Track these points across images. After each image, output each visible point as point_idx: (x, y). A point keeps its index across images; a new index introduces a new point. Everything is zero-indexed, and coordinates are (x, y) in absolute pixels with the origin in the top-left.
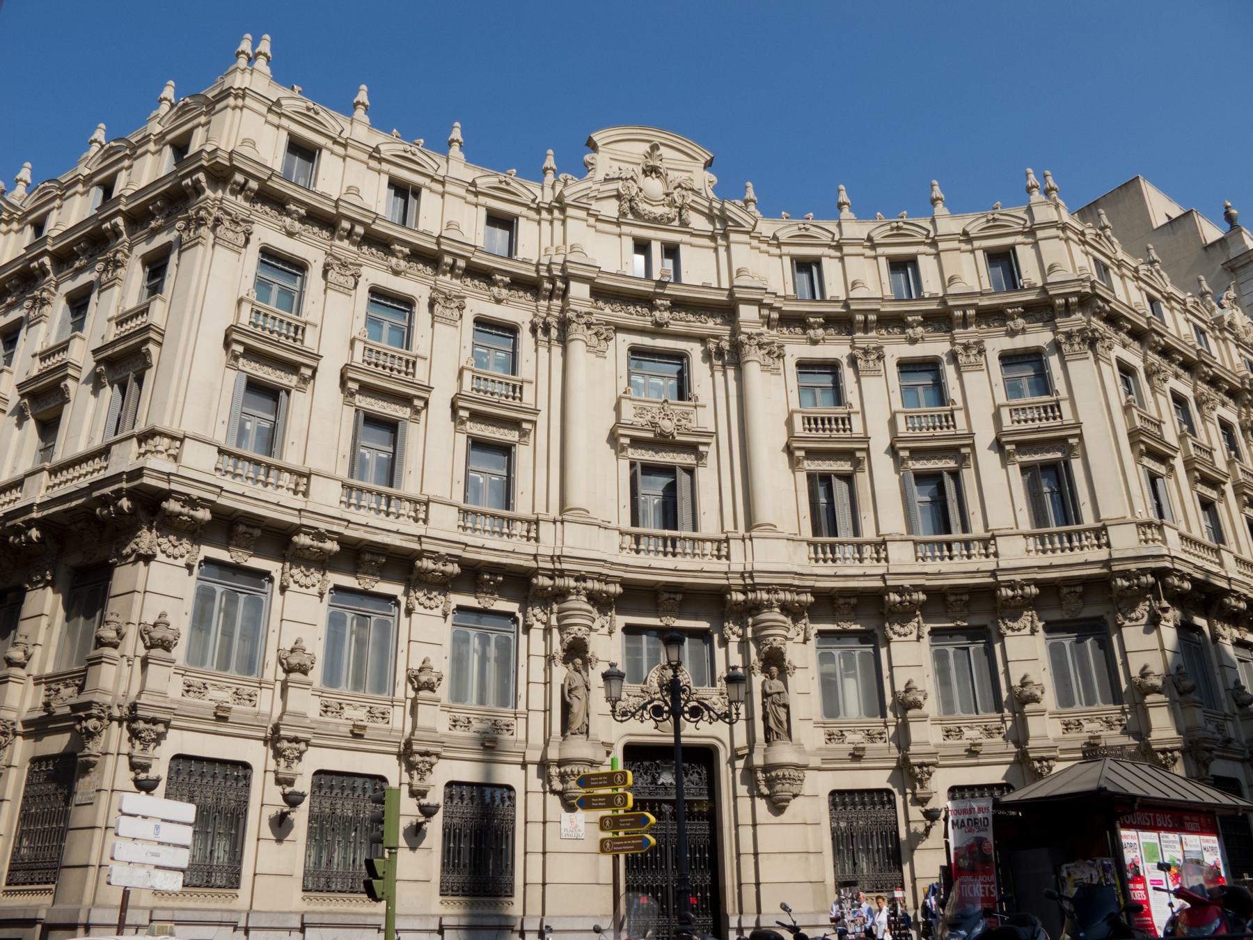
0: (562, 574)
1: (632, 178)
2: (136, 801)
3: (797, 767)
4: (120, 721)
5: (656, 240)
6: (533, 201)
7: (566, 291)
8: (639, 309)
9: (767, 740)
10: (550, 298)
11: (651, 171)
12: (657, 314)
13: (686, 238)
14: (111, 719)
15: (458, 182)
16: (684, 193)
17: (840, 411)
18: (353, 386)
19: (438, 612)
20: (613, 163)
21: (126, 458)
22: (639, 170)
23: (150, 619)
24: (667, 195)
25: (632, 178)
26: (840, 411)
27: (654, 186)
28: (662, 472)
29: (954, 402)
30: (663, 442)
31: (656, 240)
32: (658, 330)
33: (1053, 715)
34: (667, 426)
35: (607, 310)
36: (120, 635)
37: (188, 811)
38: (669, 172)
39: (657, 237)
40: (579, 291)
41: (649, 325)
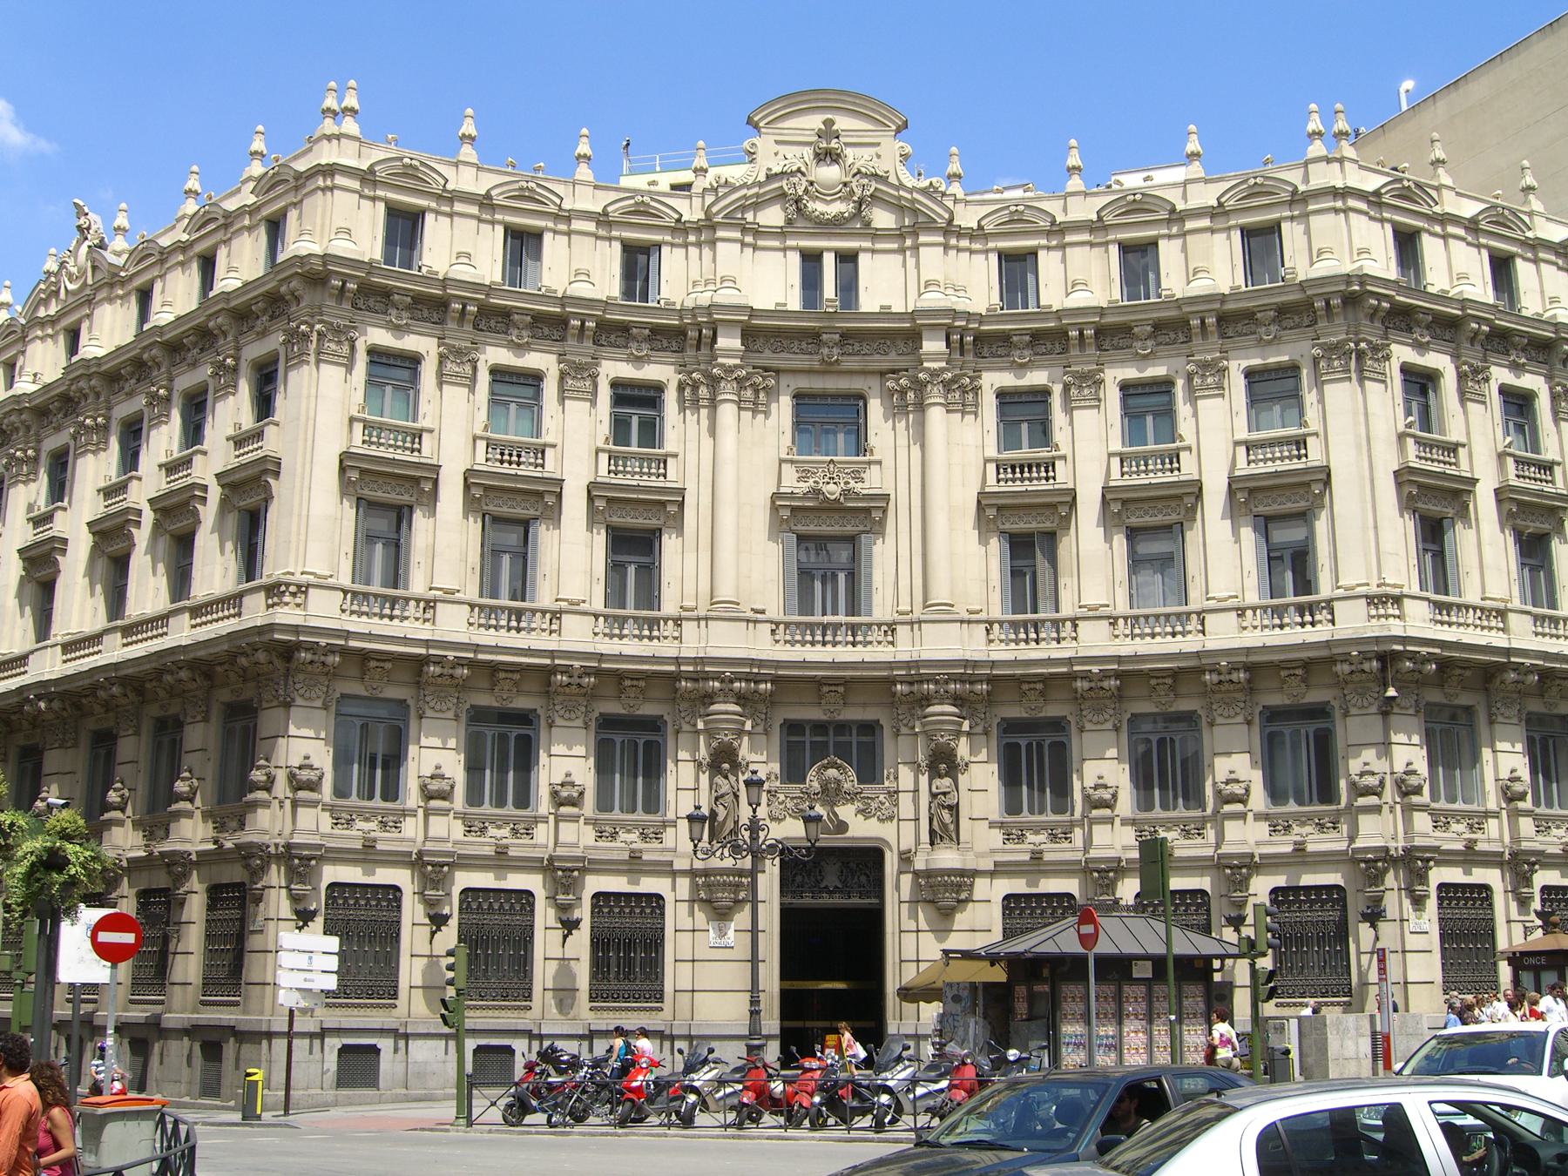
0: (707, 677)
1: (799, 170)
2: (289, 937)
3: (962, 873)
4: (278, 858)
5: (829, 250)
6: (678, 221)
7: (714, 340)
8: (804, 345)
9: (932, 844)
10: (698, 348)
11: (828, 156)
12: (825, 351)
13: (867, 244)
14: (270, 855)
15: (586, 215)
16: (865, 181)
17: (1043, 453)
18: (477, 493)
19: (579, 722)
20: (783, 149)
21: (256, 612)
22: (808, 153)
23: (295, 761)
24: (845, 184)
25: (799, 170)
26: (1043, 453)
27: (830, 173)
28: (828, 542)
29: (1182, 439)
30: (831, 508)
31: (829, 250)
32: (829, 368)
33: (1259, 817)
34: (832, 490)
35: (767, 353)
36: (271, 780)
37: (333, 943)
38: (849, 151)
39: (829, 245)
40: (729, 342)
41: (817, 365)
